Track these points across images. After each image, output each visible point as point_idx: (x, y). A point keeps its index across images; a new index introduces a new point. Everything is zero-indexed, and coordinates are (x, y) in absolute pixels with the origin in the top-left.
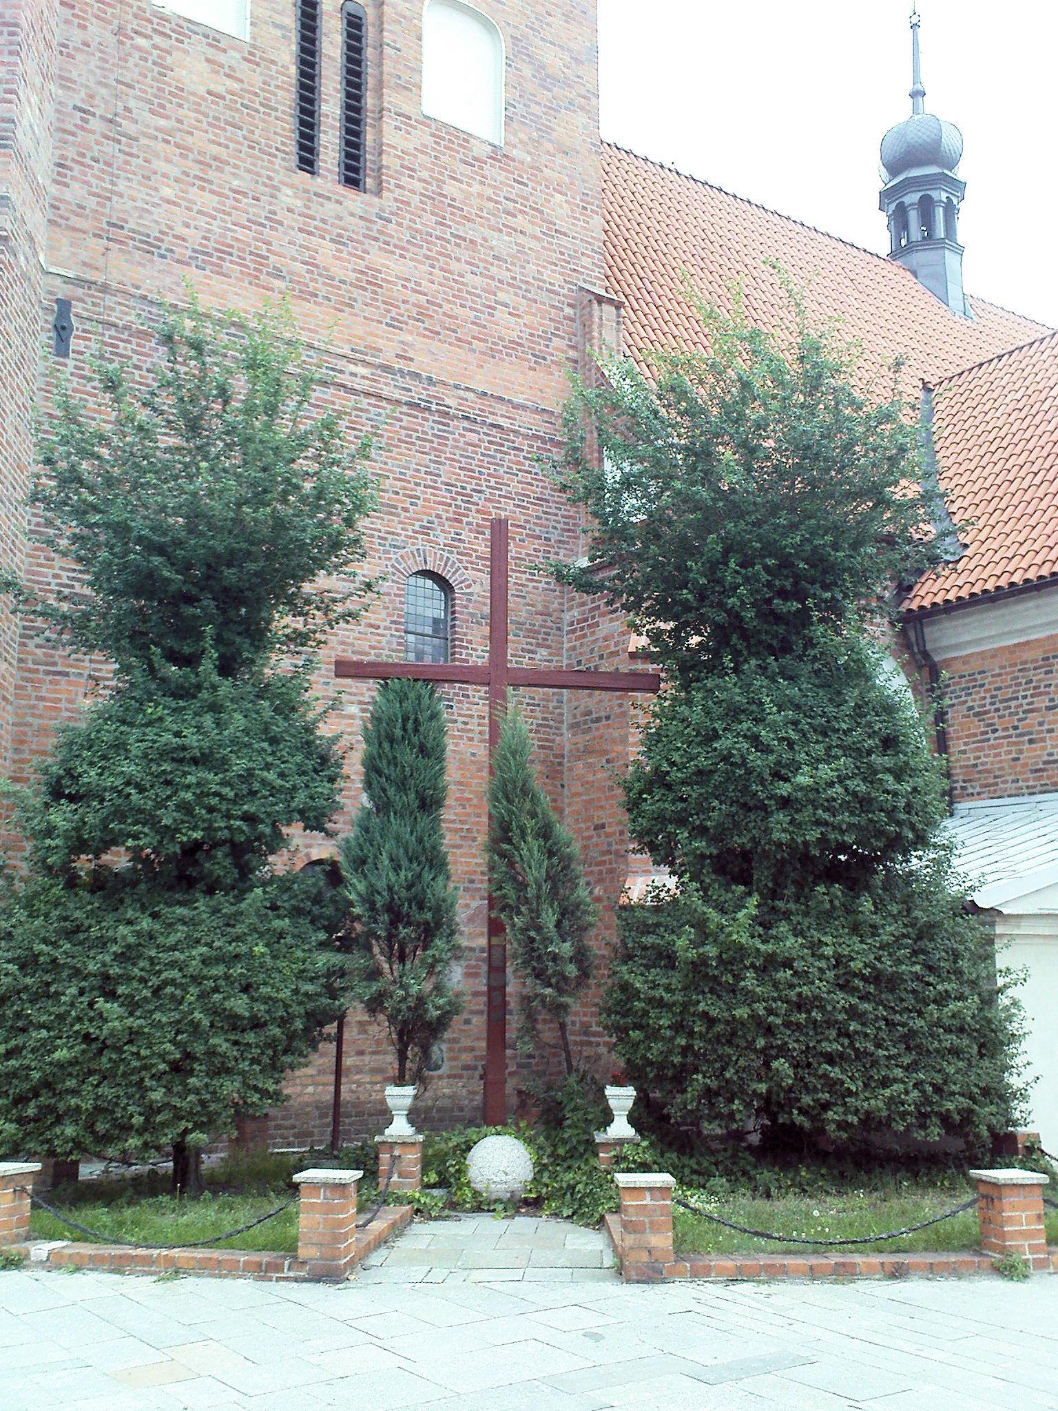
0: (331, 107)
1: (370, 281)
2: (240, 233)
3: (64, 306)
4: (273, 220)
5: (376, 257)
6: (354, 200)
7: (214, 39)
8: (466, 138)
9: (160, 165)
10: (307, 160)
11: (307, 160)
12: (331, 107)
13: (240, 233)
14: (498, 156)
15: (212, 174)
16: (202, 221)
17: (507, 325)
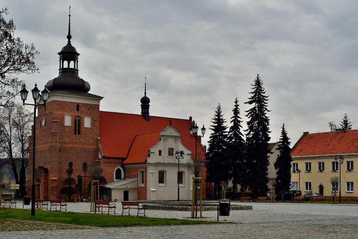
0: (77, 129)
1: (80, 142)
2: (71, 141)
3: (60, 149)
4: (73, 139)
5: (81, 140)
6: (79, 136)
7: (69, 127)
8: (88, 128)
9: (65, 137)
10: (75, 133)
12: (77, 129)
13: (71, 141)
14: (90, 128)
15: (68, 137)
16: (68, 141)
17: (91, 142)
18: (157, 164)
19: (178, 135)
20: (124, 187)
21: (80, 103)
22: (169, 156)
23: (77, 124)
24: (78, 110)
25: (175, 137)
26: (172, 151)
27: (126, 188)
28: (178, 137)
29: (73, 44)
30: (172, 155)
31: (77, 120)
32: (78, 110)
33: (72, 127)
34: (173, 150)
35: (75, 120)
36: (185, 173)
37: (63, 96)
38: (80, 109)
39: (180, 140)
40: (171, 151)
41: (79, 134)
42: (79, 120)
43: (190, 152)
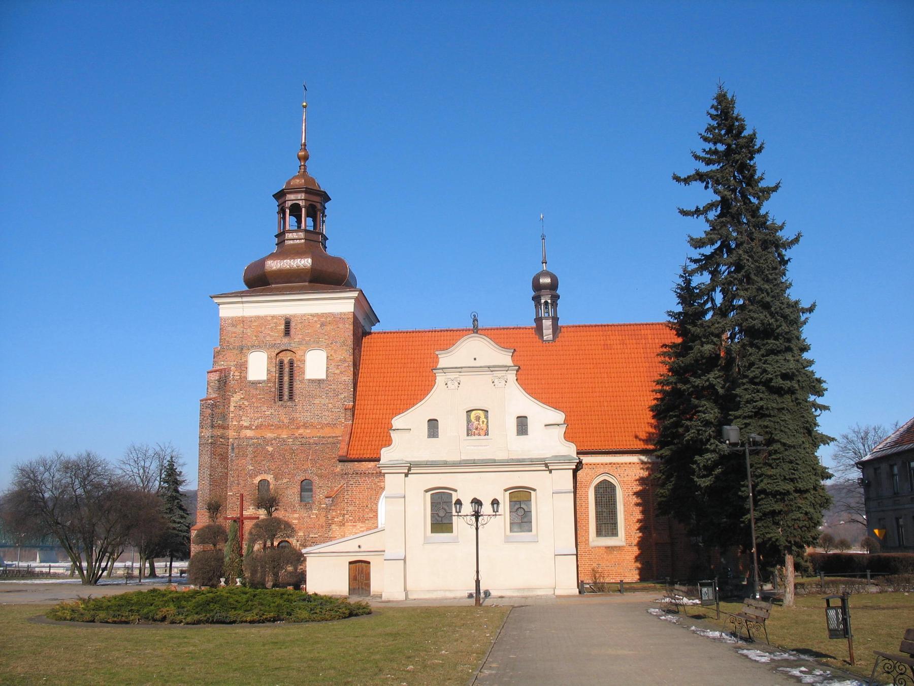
6: (289, 403)
11: (281, 399)
18: (409, 469)
19: (505, 358)
20: (352, 546)
21: (294, 316)
22: (469, 438)
23: (287, 370)
24: (287, 332)
25: (491, 368)
26: (483, 418)
27: (358, 550)
28: (506, 368)
29: (313, 170)
30: (482, 432)
31: (286, 361)
32: (287, 332)
33: (269, 380)
34: (487, 417)
35: (281, 362)
36: (537, 490)
37: (242, 302)
38: (292, 331)
39: (512, 376)
40: (478, 418)
41: (291, 397)
42: (291, 363)
43: (559, 417)
